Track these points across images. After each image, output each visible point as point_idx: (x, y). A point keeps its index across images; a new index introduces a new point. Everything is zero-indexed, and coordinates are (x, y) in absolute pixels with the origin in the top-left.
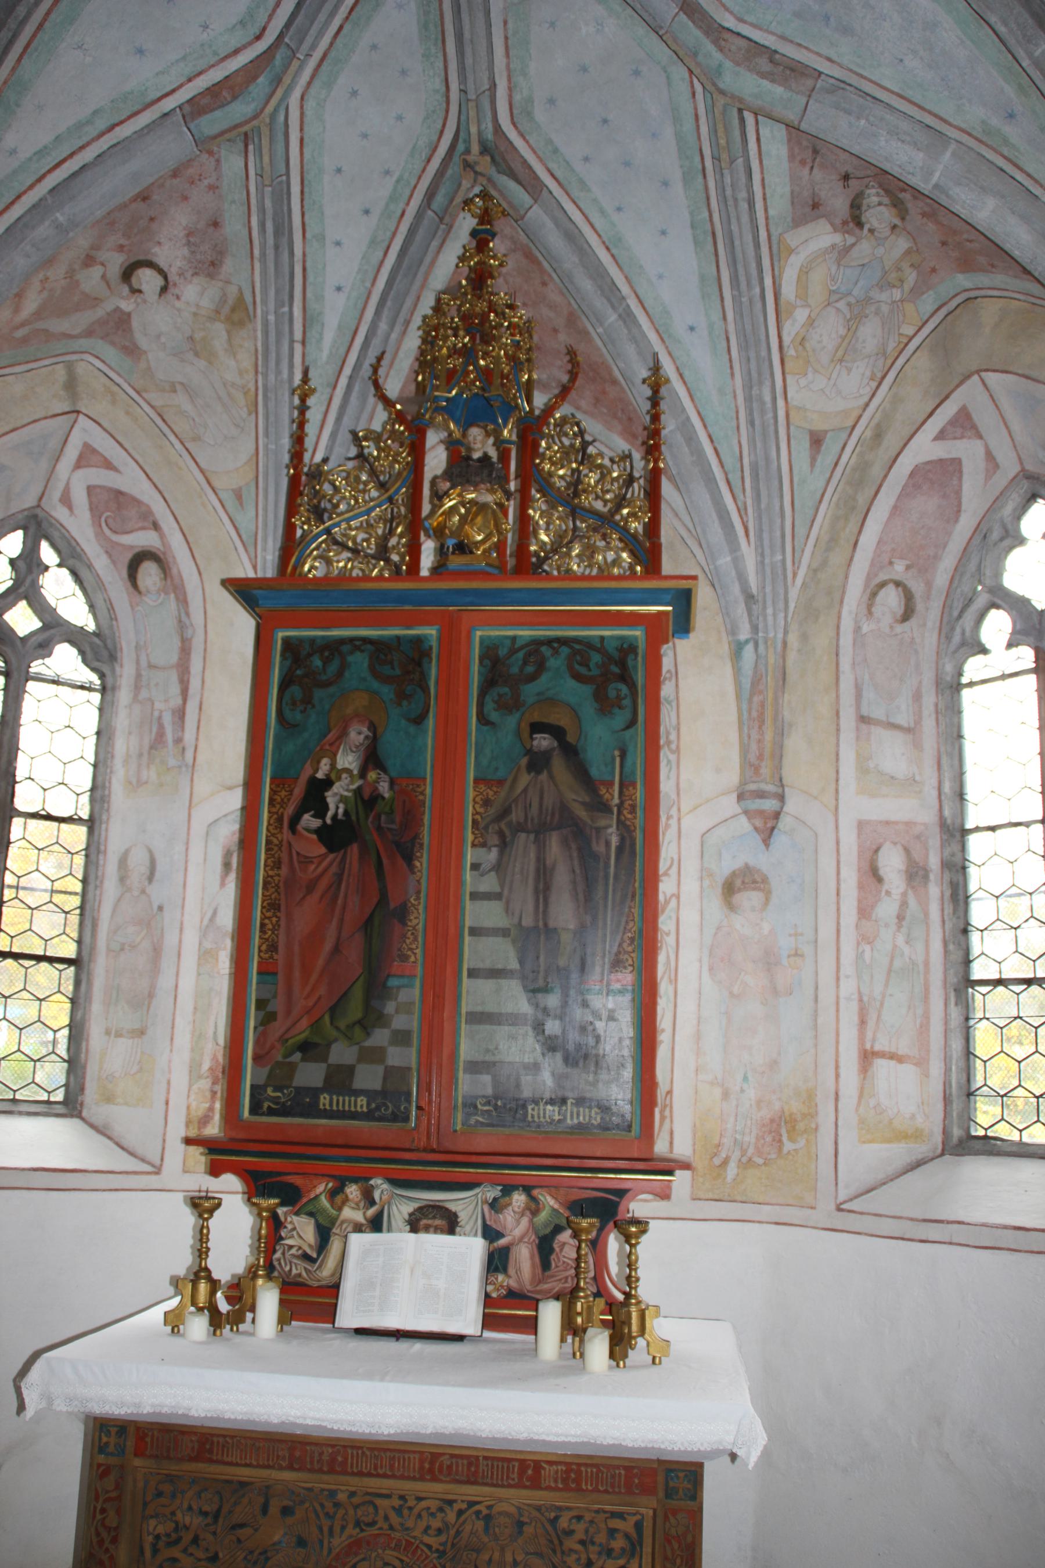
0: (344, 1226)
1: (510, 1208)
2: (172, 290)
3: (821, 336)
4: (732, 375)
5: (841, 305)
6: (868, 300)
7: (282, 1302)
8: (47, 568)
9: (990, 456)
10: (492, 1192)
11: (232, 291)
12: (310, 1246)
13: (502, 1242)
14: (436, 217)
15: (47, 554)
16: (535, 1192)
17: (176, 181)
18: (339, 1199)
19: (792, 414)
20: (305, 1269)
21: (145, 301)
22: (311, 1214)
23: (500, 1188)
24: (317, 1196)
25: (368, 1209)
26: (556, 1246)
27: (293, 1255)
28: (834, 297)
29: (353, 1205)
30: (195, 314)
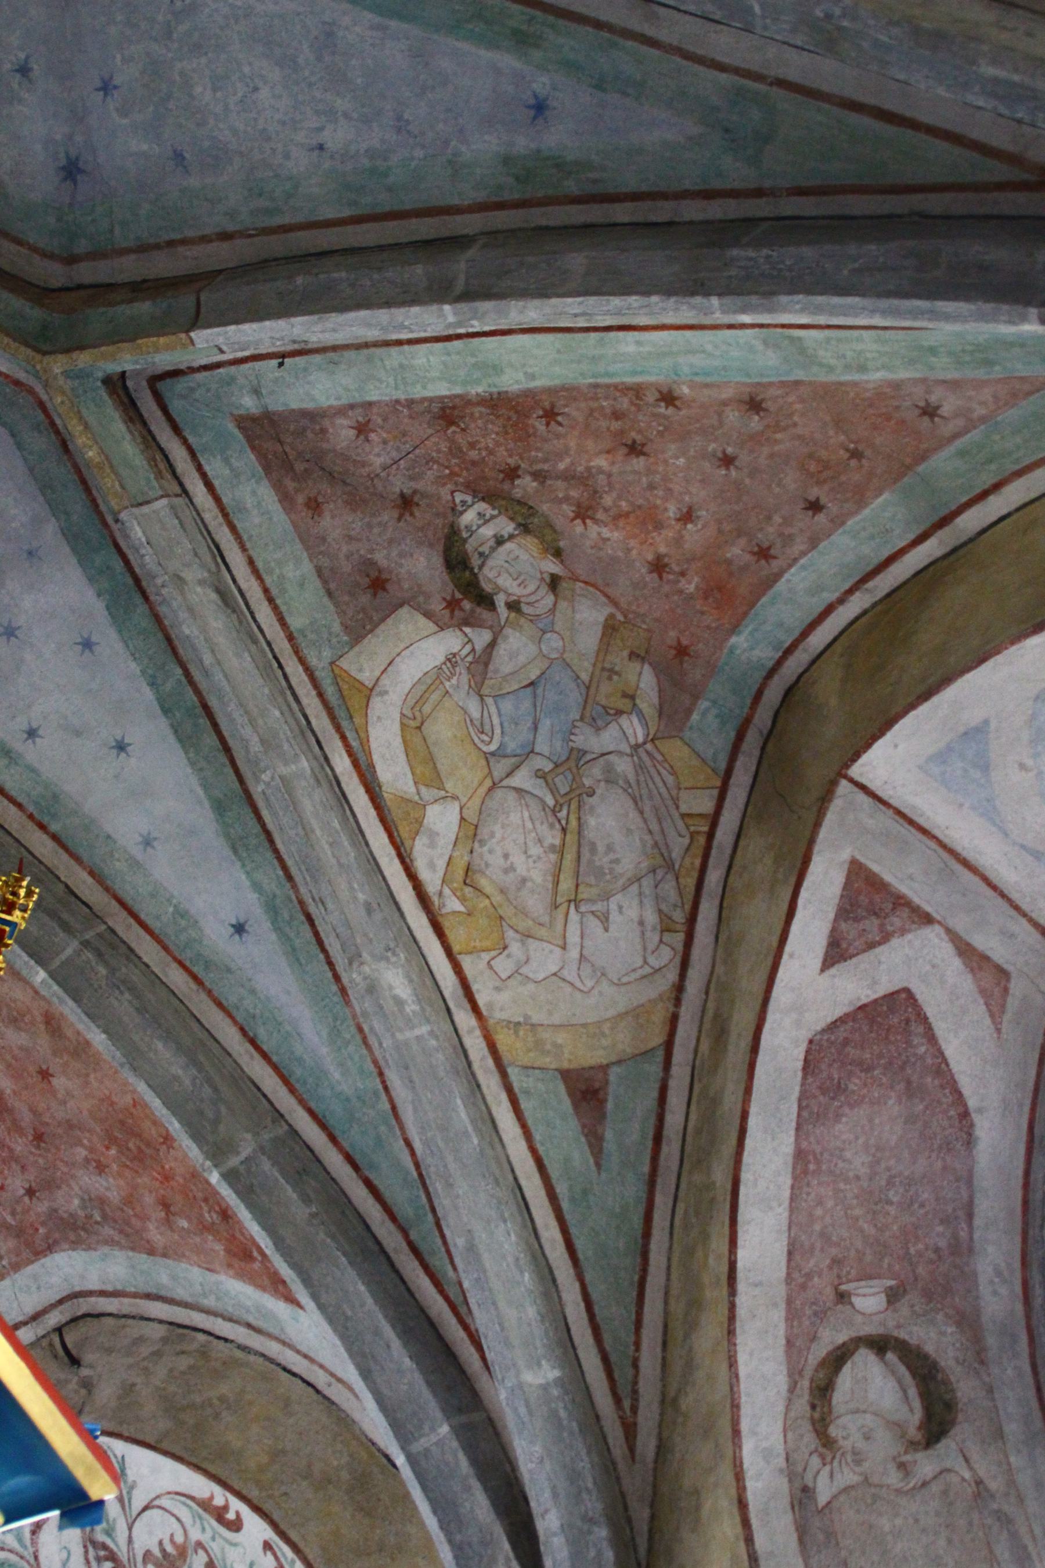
3: (506, 856)
5: (522, 779)
19: (504, 1040)
28: (500, 768)
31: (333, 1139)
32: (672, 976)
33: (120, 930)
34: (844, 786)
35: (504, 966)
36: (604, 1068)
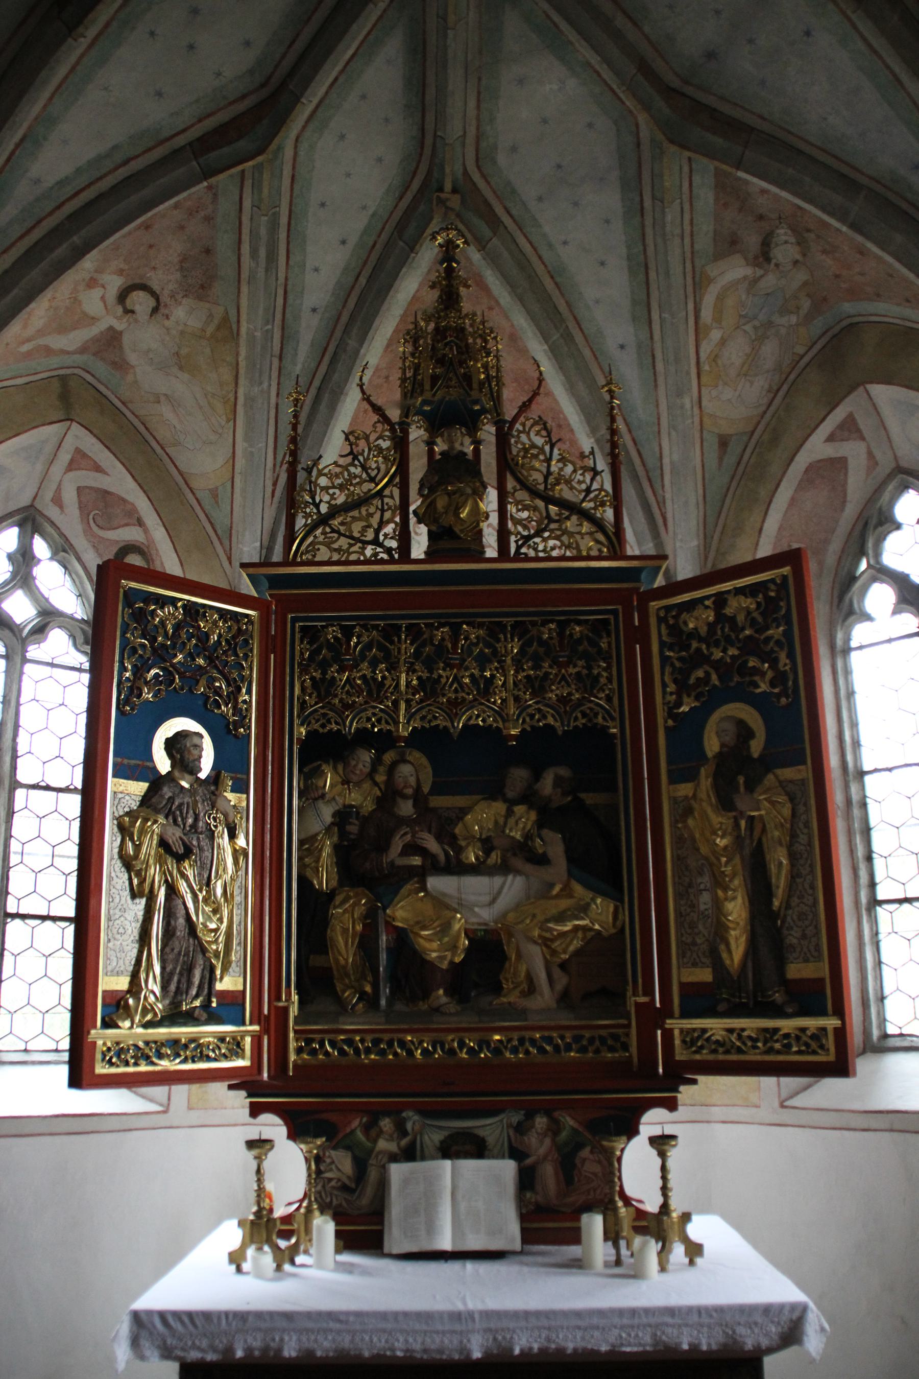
0: (380, 1157)
1: (534, 1130)
2: (163, 310)
4: (656, 386)
5: (747, 328)
6: (770, 324)
7: (338, 1234)
8: (39, 561)
9: (870, 455)
10: (516, 1118)
11: (219, 311)
12: (349, 1177)
13: (529, 1161)
14: (407, 247)
15: (40, 547)
16: (556, 1114)
17: (175, 212)
18: (373, 1133)
19: (705, 420)
20: (345, 1199)
21: (136, 321)
22: (348, 1148)
23: (523, 1112)
24: (353, 1132)
25: (401, 1139)
26: (577, 1161)
27: (333, 1187)
29: (387, 1137)
30: (182, 333)
31: (630, 431)
32: (763, 408)
33: (570, 327)
34: (861, 389)
35: (714, 393)
36: (732, 435)
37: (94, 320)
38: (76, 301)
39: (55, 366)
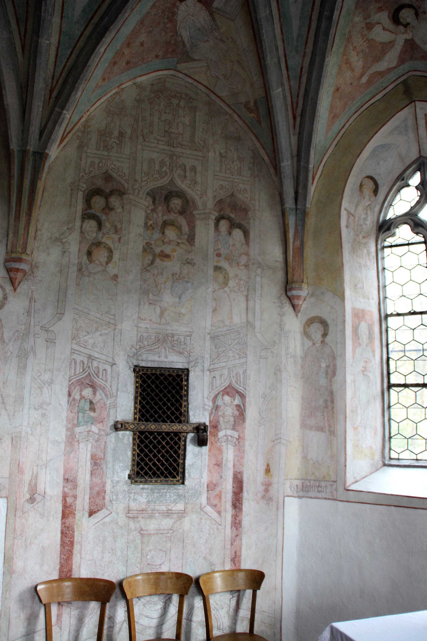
37: (392, 43)
38: (370, 41)
39: (394, 78)
